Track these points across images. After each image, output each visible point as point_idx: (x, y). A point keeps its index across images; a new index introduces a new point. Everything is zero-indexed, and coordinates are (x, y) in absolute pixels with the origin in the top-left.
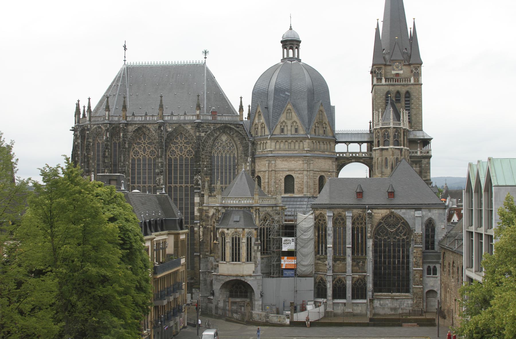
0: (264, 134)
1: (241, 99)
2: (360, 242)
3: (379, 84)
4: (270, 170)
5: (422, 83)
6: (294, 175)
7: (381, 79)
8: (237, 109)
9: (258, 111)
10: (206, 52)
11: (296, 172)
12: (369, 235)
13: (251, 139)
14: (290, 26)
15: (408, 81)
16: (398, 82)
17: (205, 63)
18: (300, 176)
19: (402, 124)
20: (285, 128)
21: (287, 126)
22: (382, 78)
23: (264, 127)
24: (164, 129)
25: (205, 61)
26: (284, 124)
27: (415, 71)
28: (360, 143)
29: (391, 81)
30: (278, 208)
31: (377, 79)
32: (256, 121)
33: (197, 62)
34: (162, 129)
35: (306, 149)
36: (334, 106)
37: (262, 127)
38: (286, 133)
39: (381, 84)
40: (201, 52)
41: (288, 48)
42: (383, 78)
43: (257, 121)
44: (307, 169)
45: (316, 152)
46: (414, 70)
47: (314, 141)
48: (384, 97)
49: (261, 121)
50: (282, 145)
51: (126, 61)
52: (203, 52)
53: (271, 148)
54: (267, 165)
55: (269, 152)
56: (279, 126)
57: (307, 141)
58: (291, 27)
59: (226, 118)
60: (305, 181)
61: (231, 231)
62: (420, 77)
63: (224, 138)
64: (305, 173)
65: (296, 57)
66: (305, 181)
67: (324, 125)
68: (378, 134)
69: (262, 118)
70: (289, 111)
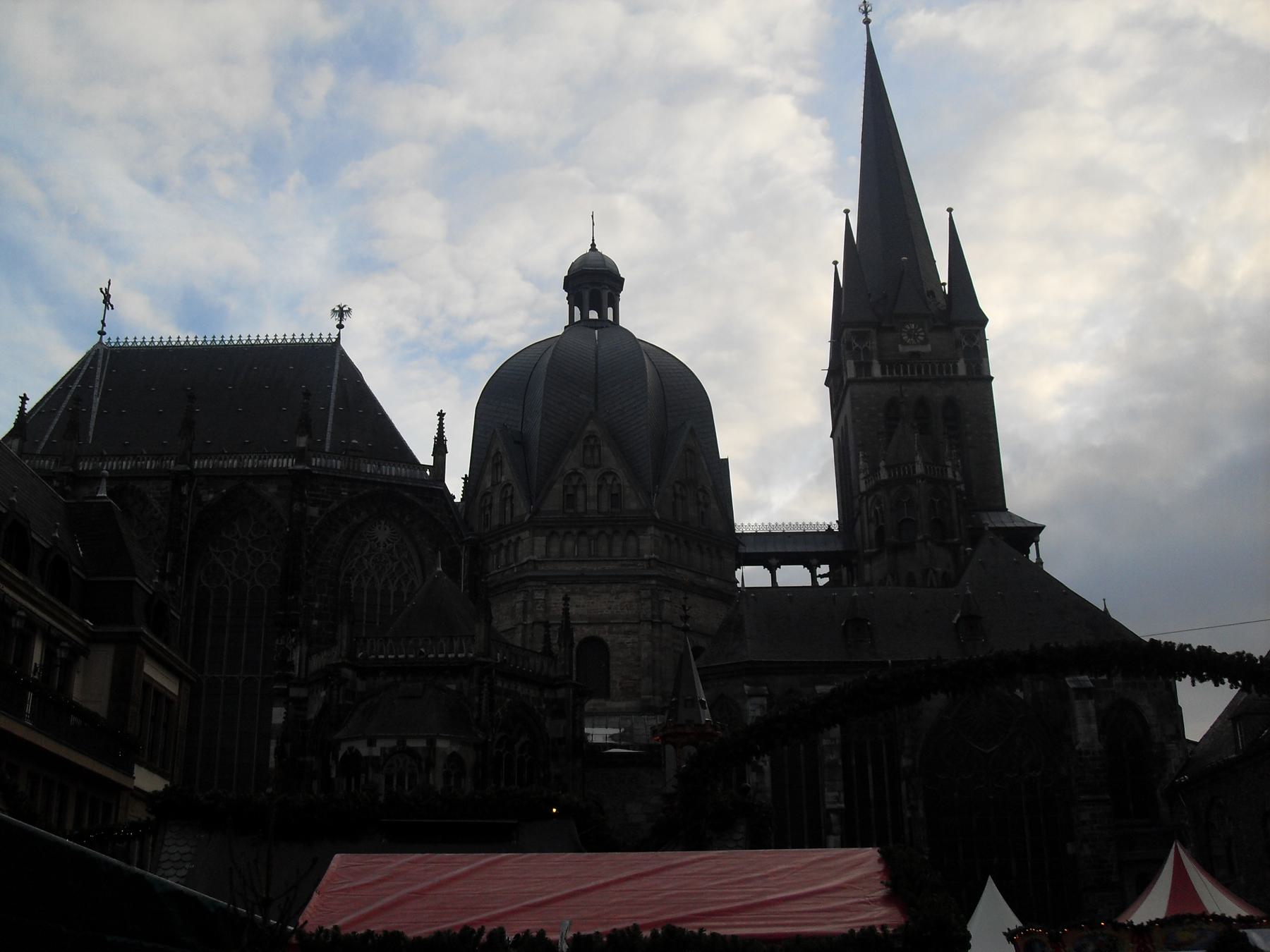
0: (512, 515)
1: (441, 420)
2: (872, 796)
3: (863, 378)
4: (529, 622)
5: (992, 375)
6: (605, 636)
7: (868, 366)
8: (425, 457)
9: (492, 454)
10: (341, 309)
11: (614, 629)
12: (905, 762)
13: (470, 537)
14: (591, 243)
15: (948, 372)
16: (919, 371)
17: (338, 339)
18: (629, 640)
19: (950, 471)
20: (580, 494)
21: (585, 486)
22: (871, 363)
23: (512, 497)
24: (189, 493)
25: (339, 335)
26: (575, 481)
27: (967, 344)
28: (809, 561)
29: (898, 372)
30: (561, 693)
31: (858, 366)
32: (487, 481)
33: (316, 336)
34: (185, 492)
35: (646, 556)
36: (727, 460)
37: (506, 499)
38: (581, 509)
39: (869, 378)
40: (330, 312)
41: (586, 295)
42: (875, 362)
43: (489, 484)
44: (653, 616)
45: (678, 571)
46: (963, 340)
47: (673, 536)
48: (881, 414)
49: (503, 480)
50: (569, 544)
51: (105, 334)
52: (334, 310)
53: (533, 554)
54: (519, 606)
55: (525, 566)
56: (558, 487)
57: (651, 530)
58: (593, 245)
59: (391, 470)
60: (644, 655)
61: (383, 749)
62: (984, 359)
63: (382, 533)
64: (646, 628)
65: (610, 317)
66: (644, 655)
67: (701, 495)
68: (877, 508)
69: (507, 468)
70: (592, 441)
